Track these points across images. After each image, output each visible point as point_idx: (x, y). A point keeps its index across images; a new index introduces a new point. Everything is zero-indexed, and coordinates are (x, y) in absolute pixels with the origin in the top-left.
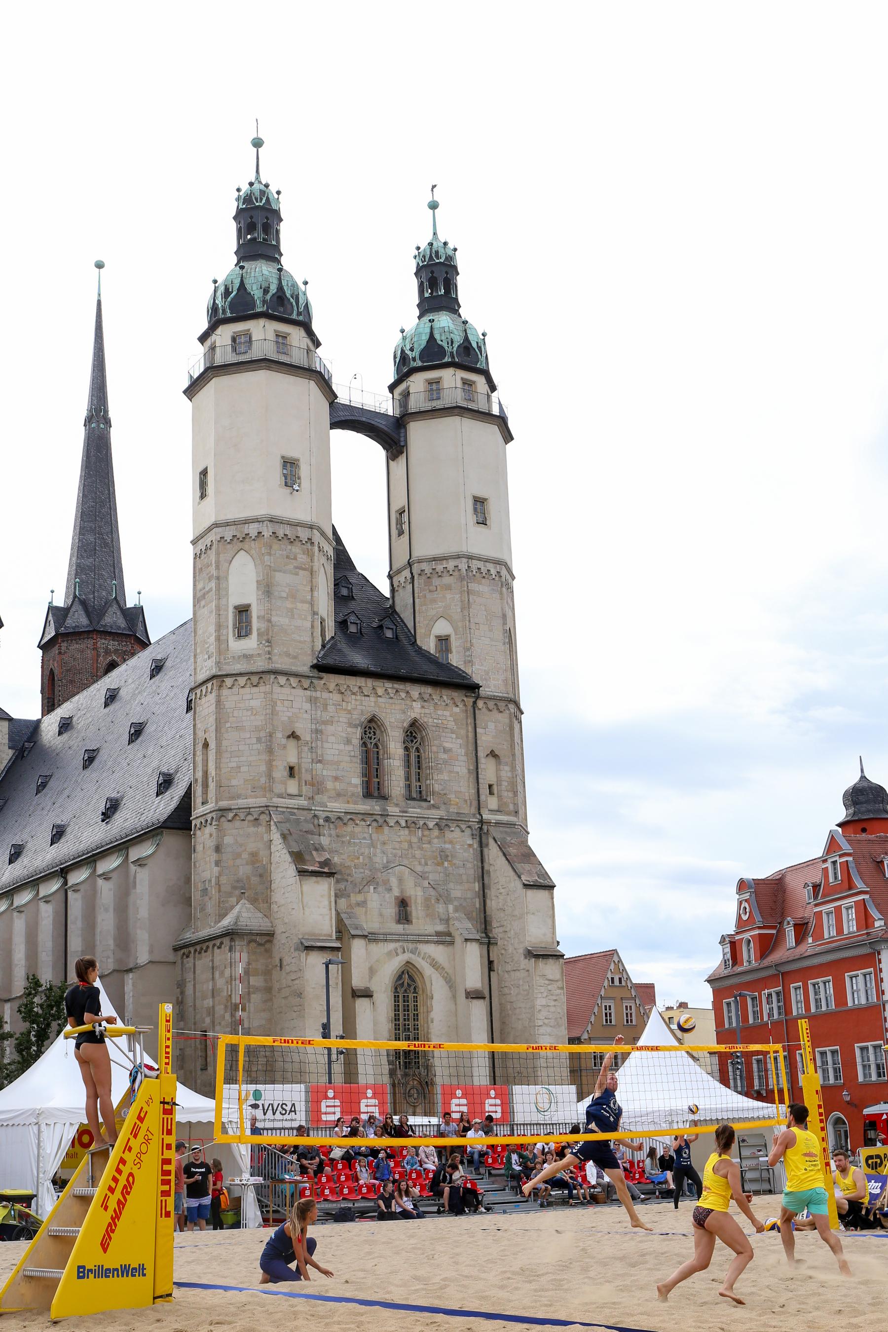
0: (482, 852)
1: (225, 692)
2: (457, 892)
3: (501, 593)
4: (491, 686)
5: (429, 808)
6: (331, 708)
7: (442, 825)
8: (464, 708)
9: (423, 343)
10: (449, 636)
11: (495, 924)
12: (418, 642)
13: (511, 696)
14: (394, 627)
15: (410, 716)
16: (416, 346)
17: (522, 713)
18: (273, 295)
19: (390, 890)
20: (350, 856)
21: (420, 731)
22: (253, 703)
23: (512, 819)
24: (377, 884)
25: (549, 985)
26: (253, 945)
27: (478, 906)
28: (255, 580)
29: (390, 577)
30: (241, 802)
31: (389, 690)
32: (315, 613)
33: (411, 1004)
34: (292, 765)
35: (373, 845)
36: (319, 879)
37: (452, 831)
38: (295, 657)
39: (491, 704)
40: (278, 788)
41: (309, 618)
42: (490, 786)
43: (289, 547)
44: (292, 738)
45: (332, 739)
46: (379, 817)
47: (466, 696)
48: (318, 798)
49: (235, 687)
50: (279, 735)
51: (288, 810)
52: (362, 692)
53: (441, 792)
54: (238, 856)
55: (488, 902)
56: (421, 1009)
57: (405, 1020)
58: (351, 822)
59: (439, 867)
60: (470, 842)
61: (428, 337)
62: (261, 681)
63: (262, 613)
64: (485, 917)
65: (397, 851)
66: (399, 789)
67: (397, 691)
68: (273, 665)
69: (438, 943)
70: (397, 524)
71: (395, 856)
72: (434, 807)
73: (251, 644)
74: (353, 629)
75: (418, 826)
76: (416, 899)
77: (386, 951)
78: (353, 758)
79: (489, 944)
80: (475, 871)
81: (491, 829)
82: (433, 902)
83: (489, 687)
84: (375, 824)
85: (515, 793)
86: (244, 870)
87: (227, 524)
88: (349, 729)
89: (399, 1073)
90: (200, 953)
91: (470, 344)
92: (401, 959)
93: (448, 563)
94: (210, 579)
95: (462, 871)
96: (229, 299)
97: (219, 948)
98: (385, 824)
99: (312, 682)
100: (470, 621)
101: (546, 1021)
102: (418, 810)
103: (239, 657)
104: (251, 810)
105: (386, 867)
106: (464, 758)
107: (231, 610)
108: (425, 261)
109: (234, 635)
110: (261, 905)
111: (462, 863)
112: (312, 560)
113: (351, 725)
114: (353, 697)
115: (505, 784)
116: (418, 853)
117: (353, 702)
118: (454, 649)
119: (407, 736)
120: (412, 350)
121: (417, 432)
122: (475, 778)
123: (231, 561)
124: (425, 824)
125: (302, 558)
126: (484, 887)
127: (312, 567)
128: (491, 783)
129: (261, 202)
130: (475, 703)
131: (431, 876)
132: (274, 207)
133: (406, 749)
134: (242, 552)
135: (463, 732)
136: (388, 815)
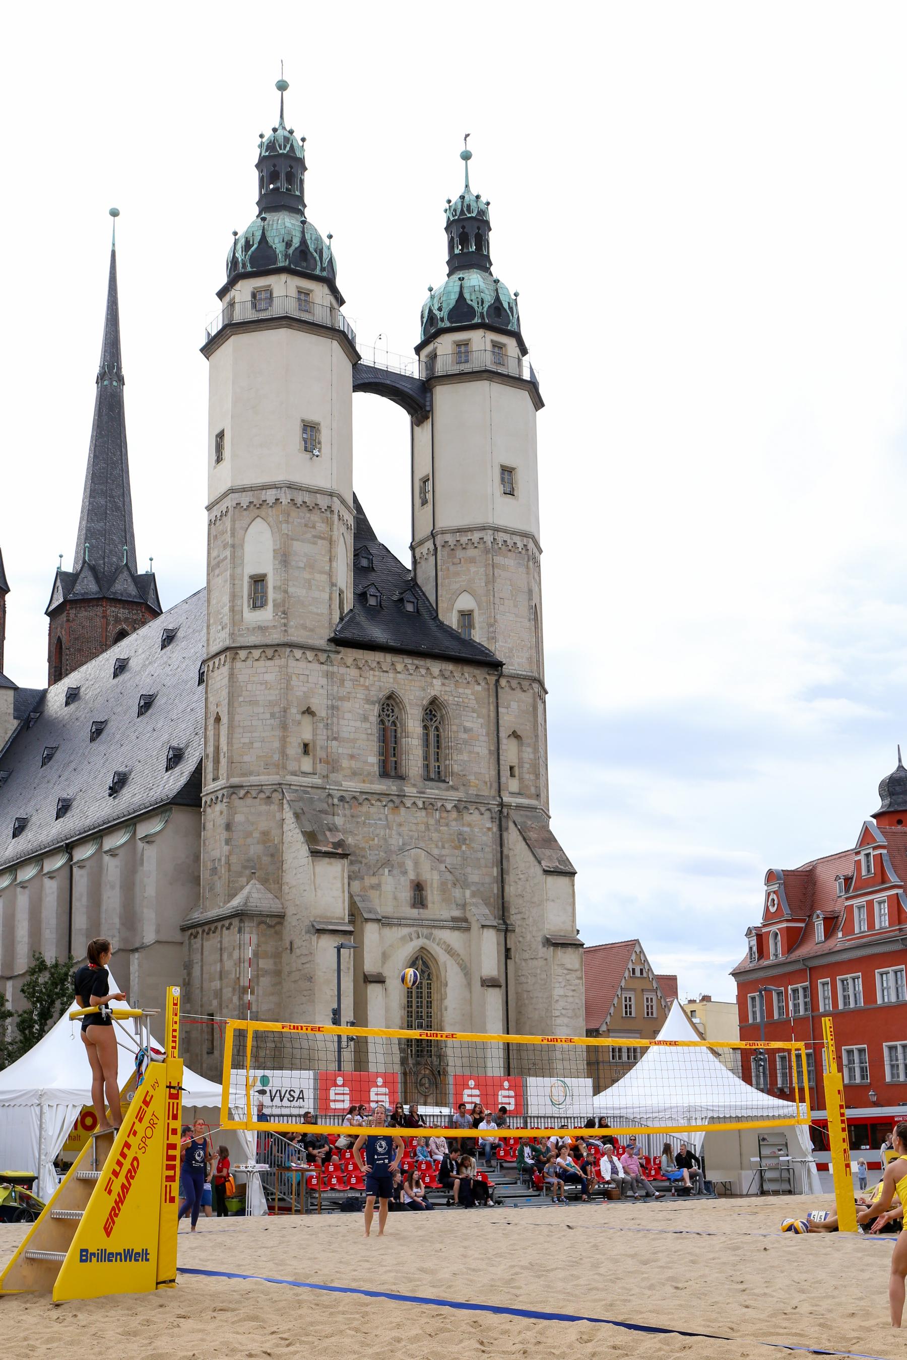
0: (501, 836)
1: (239, 665)
2: (474, 876)
3: (528, 567)
4: (515, 664)
5: (447, 789)
6: (348, 684)
7: (460, 808)
8: (487, 687)
9: (452, 303)
10: (472, 611)
11: (513, 911)
12: (440, 617)
13: (535, 675)
14: (415, 601)
15: (430, 694)
16: (444, 305)
17: (547, 693)
18: (296, 249)
19: (405, 873)
20: (364, 837)
21: (440, 710)
22: (270, 677)
23: (533, 802)
24: (392, 866)
25: (567, 974)
26: (263, 926)
27: (496, 891)
28: (271, 549)
29: (412, 548)
30: (254, 780)
31: (409, 666)
32: (333, 585)
33: (425, 991)
34: (306, 741)
35: (388, 826)
36: (332, 860)
38: (312, 630)
39: (514, 683)
40: (292, 766)
41: (328, 590)
42: (511, 768)
43: (308, 515)
44: (307, 714)
45: (348, 716)
46: (396, 797)
47: (489, 674)
48: (333, 776)
49: (249, 659)
50: (294, 710)
51: (302, 788)
52: (381, 668)
53: (461, 773)
54: (249, 834)
55: (507, 888)
56: (435, 996)
57: (418, 1007)
58: (366, 802)
59: (456, 851)
60: (489, 825)
61: (457, 296)
62: (276, 654)
63: (279, 584)
64: (503, 903)
65: (414, 833)
66: (417, 769)
67: (417, 667)
68: (289, 638)
69: (453, 928)
70: (420, 493)
71: (411, 838)
72: (453, 788)
73: (266, 615)
74: (372, 602)
75: (435, 808)
76: (432, 884)
77: (400, 936)
78: (369, 736)
79: (506, 931)
80: (493, 856)
81: (512, 812)
82: (449, 886)
83: (513, 665)
84: (391, 805)
85: (537, 776)
86: (255, 849)
87: (244, 490)
88: (367, 706)
89: (410, 1061)
90: (208, 934)
91: (502, 304)
92: (416, 944)
93: (473, 535)
94: (225, 547)
95: (480, 855)
96: (250, 253)
97: (228, 928)
98: (402, 805)
99: (328, 656)
100: (494, 596)
101: (564, 1012)
102: (436, 792)
103: (254, 629)
104: (264, 787)
105: (402, 850)
106: (485, 738)
107: (246, 579)
108: (456, 215)
109: (249, 606)
110: (272, 886)
111: (480, 847)
112: (331, 530)
113: (368, 701)
114: (371, 672)
115: (527, 766)
116: (435, 836)
117: (371, 678)
118: (477, 625)
119: (427, 714)
120: (440, 309)
121: (443, 396)
122: (496, 759)
123: (247, 529)
124: (443, 805)
125: (321, 527)
126: (502, 872)
127: (331, 536)
128: (512, 764)
129: (285, 149)
130: (497, 681)
131: (448, 860)
132: (299, 155)
133: (425, 727)
134: (259, 520)
135: (484, 711)
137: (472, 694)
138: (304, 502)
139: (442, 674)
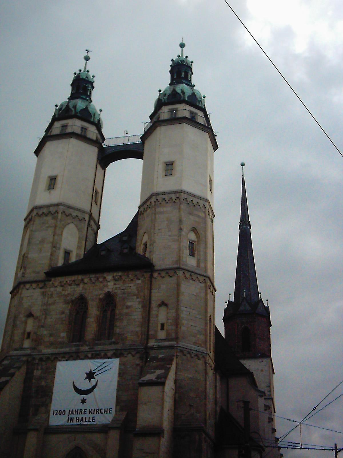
5: (110, 344)
23: (173, 343)
31: (92, 279)
37: (126, 357)
39: (163, 274)
42: (163, 325)
60: (138, 362)
72: (115, 343)
88: (64, 306)
113: (66, 302)
114: (69, 287)
136: (79, 352)
138: (43, 213)
139: (115, 279)
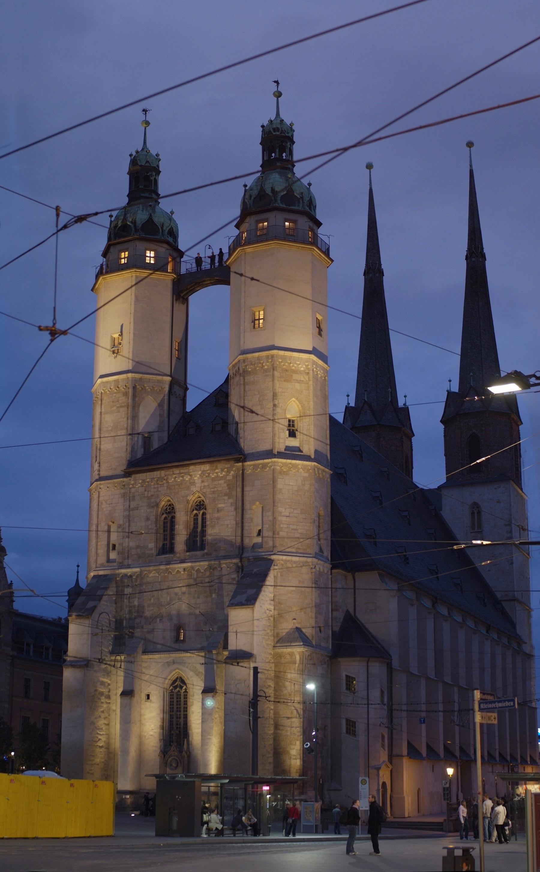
88: (149, 510)
117: (152, 490)
137: (225, 482)
